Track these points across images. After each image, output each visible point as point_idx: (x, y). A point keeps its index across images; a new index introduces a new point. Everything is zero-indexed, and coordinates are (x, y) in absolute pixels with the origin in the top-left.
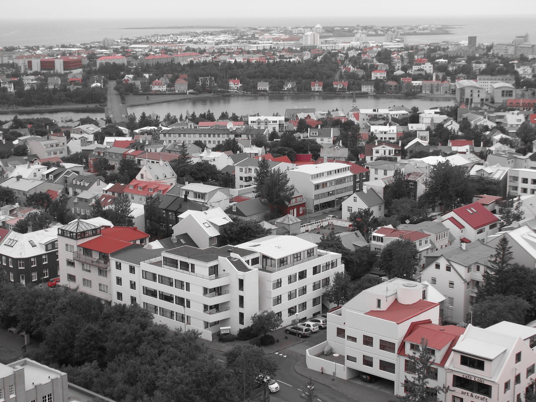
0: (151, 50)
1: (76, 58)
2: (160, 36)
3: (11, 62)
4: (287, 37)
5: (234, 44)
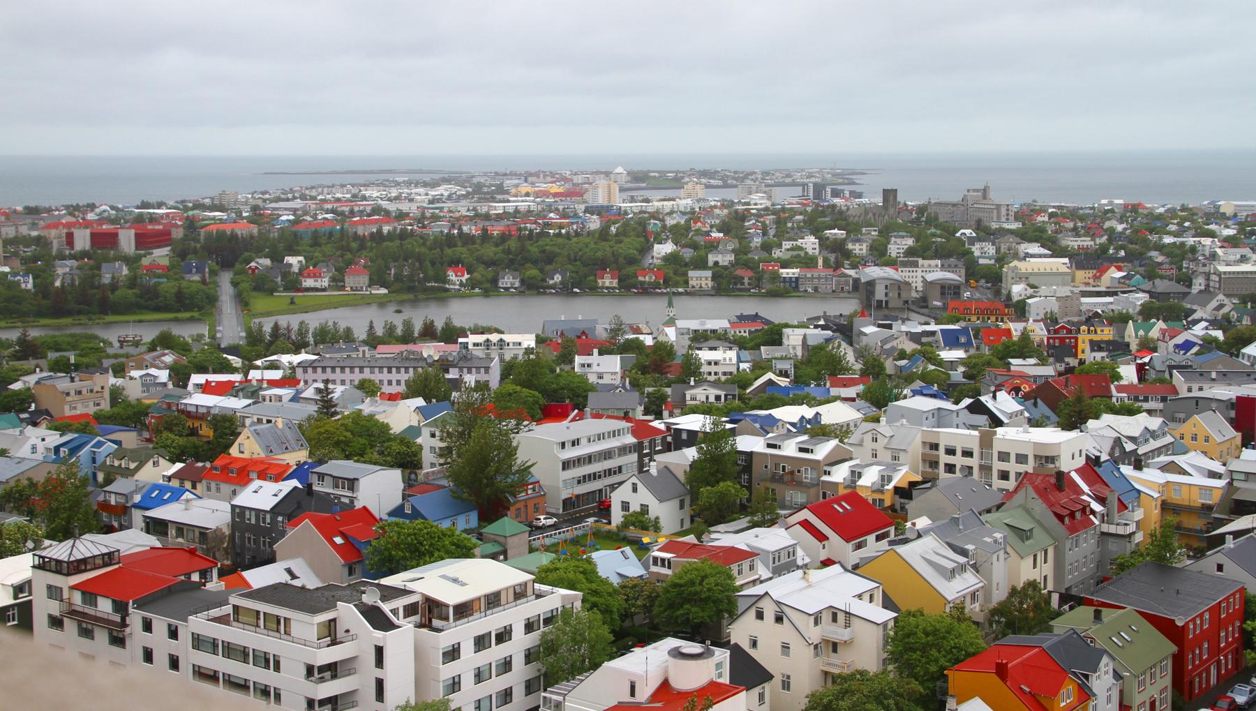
0: (306, 213)
1: (161, 227)
2: (328, 187)
3: (34, 233)
5: (464, 202)
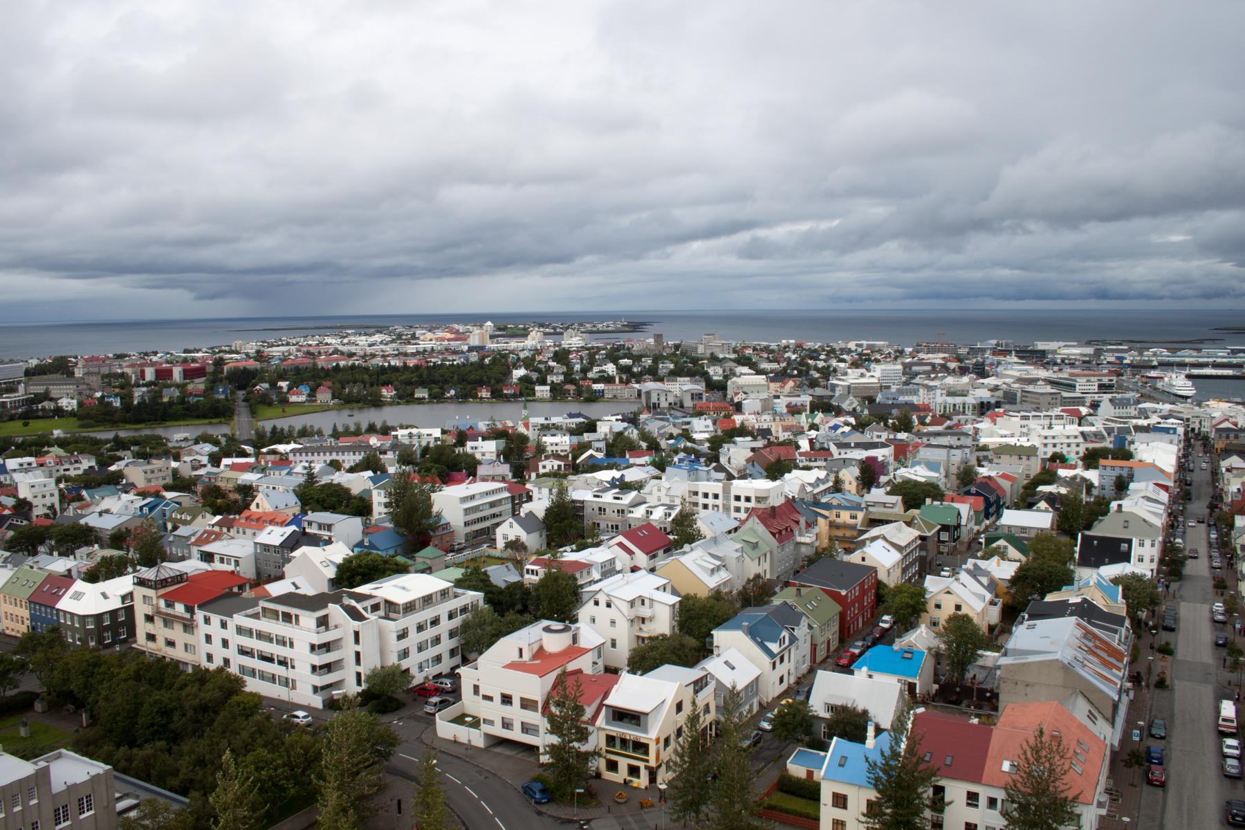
0: (290, 354)
1: (197, 365)
4: (453, 336)
5: (390, 346)
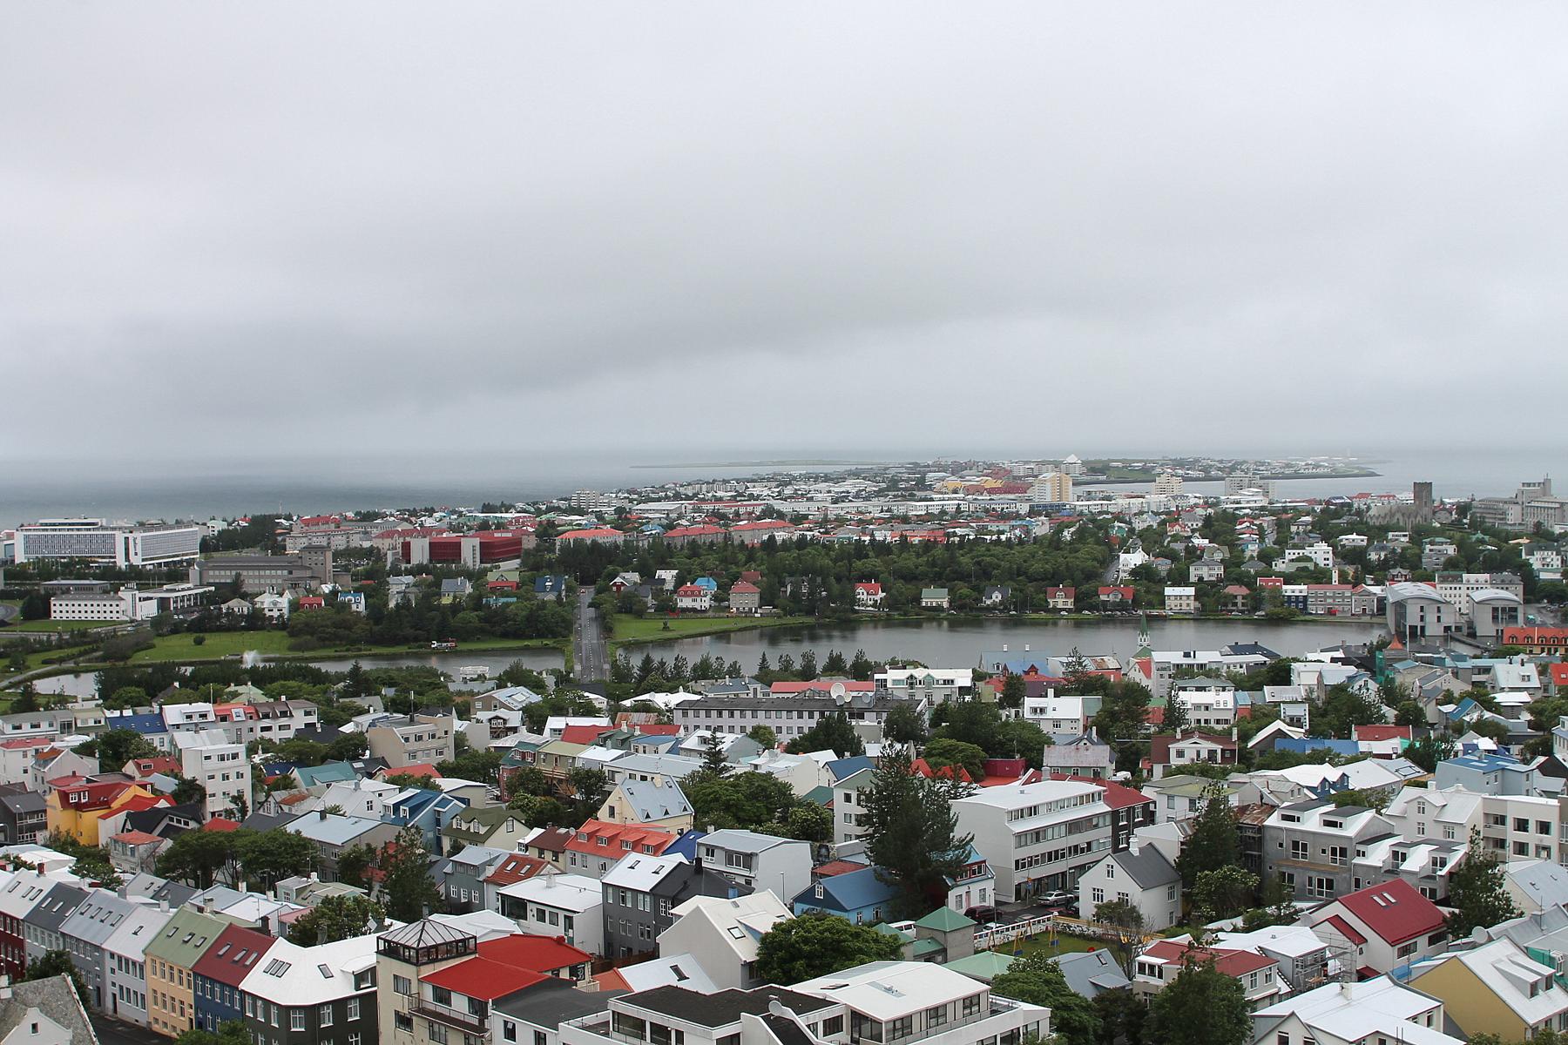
0: (680, 517)
1: (510, 535)
2: (708, 483)
3: (366, 544)
4: (999, 484)
5: (875, 501)
